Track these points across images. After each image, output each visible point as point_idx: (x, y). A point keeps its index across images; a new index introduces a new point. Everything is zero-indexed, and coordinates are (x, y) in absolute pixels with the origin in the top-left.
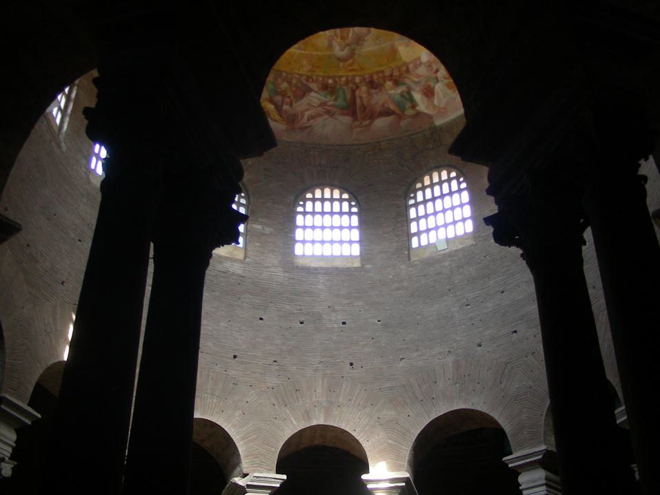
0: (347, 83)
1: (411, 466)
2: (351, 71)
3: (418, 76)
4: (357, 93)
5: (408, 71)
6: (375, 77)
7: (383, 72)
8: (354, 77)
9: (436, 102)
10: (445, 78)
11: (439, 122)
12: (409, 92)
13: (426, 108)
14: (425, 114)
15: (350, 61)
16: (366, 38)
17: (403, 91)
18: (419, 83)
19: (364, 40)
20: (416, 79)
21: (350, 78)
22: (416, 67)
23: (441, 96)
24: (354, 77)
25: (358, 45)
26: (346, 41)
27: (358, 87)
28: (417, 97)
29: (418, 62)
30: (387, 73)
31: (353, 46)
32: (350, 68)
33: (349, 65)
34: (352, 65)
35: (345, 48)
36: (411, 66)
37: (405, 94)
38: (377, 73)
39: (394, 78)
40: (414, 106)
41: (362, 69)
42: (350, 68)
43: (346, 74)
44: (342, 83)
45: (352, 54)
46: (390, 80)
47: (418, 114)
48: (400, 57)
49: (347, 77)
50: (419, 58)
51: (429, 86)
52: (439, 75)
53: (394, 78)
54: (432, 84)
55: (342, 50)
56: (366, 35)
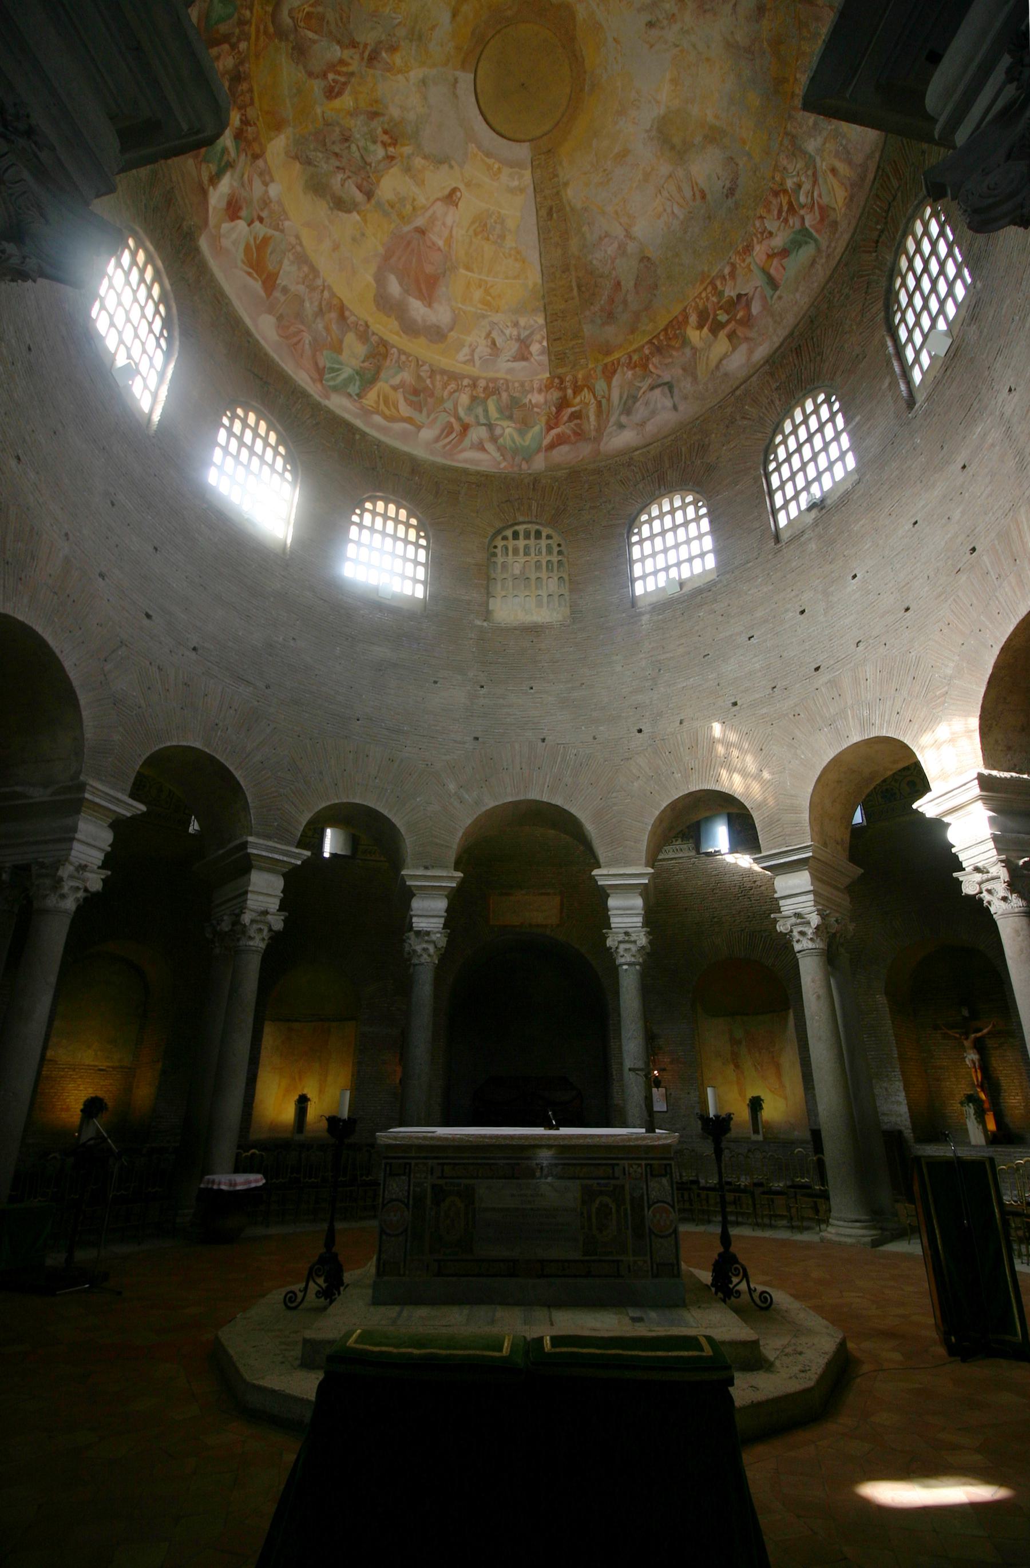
0: (242, 23)
1: (247, 520)
2: (258, 31)
3: (250, 181)
4: (226, 47)
5: (256, 157)
6: (245, 86)
7: (252, 103)
8: (248, 39)
9: (226, 226)
10: (255, 239)
11: (204, 244)
12: (230, 165)
13: (215, 208)
14: (207, 210)
15: (271, 30)
16: (301, 67)
17: (229, 154)
18: (243, 185)
19: (297, 63)
20: (246, 176)
21: (246, 28)
22: (261, 174)
23: (234, 236)
24: (248, 39)
25: (293, 48)
26: (302, 24)
27: (234, 47)
28: (226, 184)
29: (267, 178)
30: (251, 113)
31: (292, 37)
32: (262, 27)
33: (266, 27)
34: (265, 32)
35: (292, 18)
36: (260, 163)
37: (225, 158)
38: (251, 90)
39: (245, 128)
40: (215, 179)
41: (257, 56)
42: (262, 27)
43: (254, 21)
44: (243, 11)
45: (281, 34)
46: (241, 121)
47: (204, 193)
48: (271, 139)
49: (248, 22)
50: (272, 180)
51: (240, 208)
52: (257, 223)
53: (245, 128)
54: (243, 213)
55: (290, 11)
56: (305, 67)
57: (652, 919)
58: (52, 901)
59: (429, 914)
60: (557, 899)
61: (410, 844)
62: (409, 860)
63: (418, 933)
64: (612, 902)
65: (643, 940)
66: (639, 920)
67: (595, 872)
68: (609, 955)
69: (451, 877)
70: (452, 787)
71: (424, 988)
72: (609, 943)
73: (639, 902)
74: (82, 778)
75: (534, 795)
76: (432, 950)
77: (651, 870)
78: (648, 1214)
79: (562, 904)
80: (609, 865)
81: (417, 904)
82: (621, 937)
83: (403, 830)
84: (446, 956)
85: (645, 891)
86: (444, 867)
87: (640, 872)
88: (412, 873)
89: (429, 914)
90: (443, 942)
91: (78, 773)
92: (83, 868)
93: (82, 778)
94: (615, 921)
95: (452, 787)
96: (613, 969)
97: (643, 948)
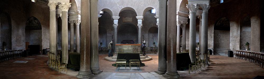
57: (143, 22)
58: (78, 24)
59: (116, 22)
60: (132, 18)
61: (113, 13)
62: (113, 15)
63: (115, 24)
64: (138, 20)
65: (142, 25)
66: (141, 23)
67: (136, 17)
68: (138, 27)
69: (119, 17)
70: (118, 5)
71: (116, 31)
72: (138, 25)
73: (141, 21)
74: (78, 11)
75: (128, 6)
76: (116, 26)
77: (143, 17)
78: (138, 50)
79: (132, 19)
80: (138, 16)
81: (114, 21)
82: (139, 25)
83: (112, 12)
84: (118, 27)
85: (142, 19)
86: (118, 16)
87: (142, 17)
88: (114, 17)
89: (116, 22)
90: (118, 25)
91: (77, 10)
92: (80, 20)
93: (78, 11)
94: (138, 23)
95: (118, 5)
96: (138, 28)
97: (142, 26)
